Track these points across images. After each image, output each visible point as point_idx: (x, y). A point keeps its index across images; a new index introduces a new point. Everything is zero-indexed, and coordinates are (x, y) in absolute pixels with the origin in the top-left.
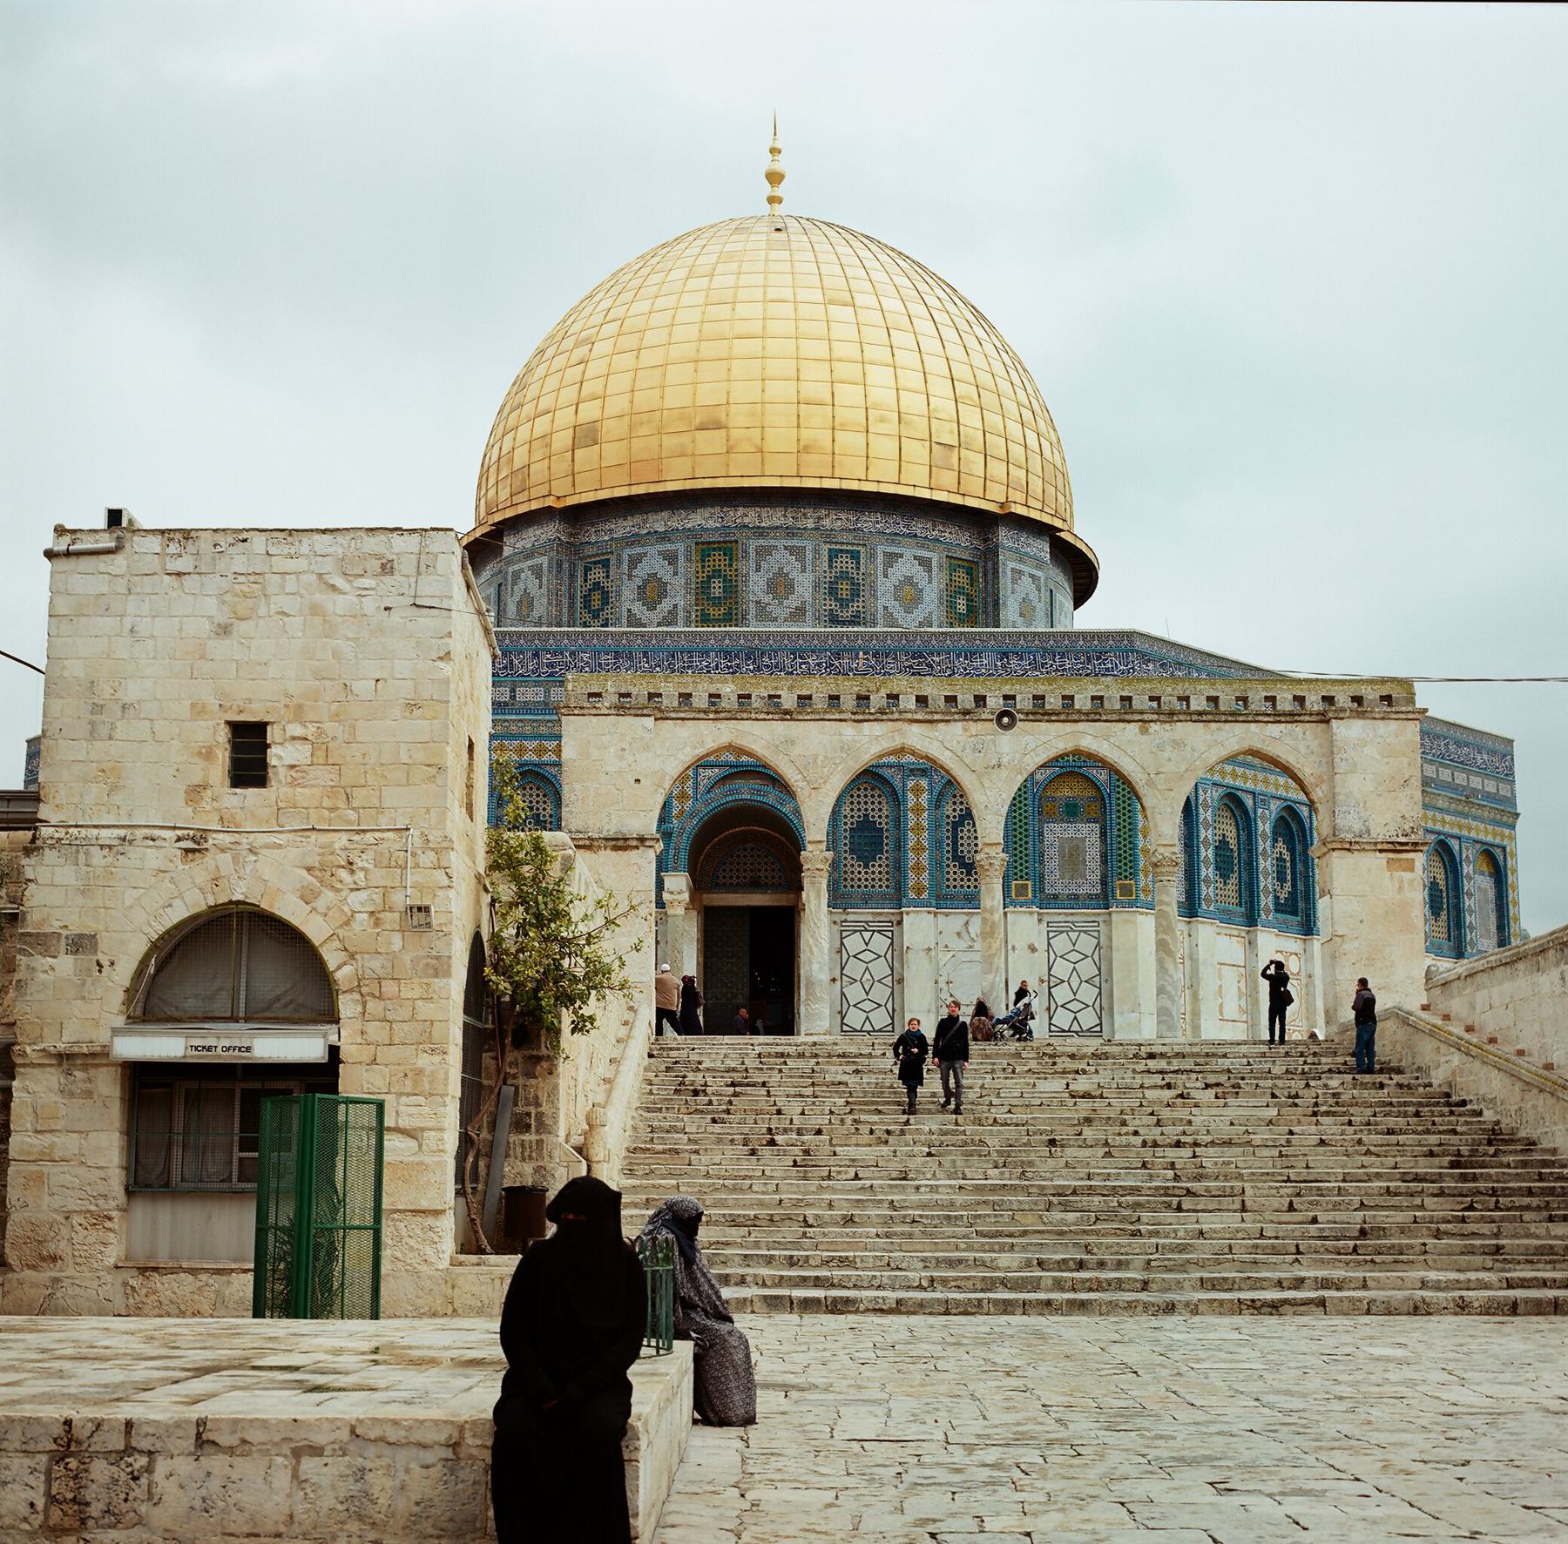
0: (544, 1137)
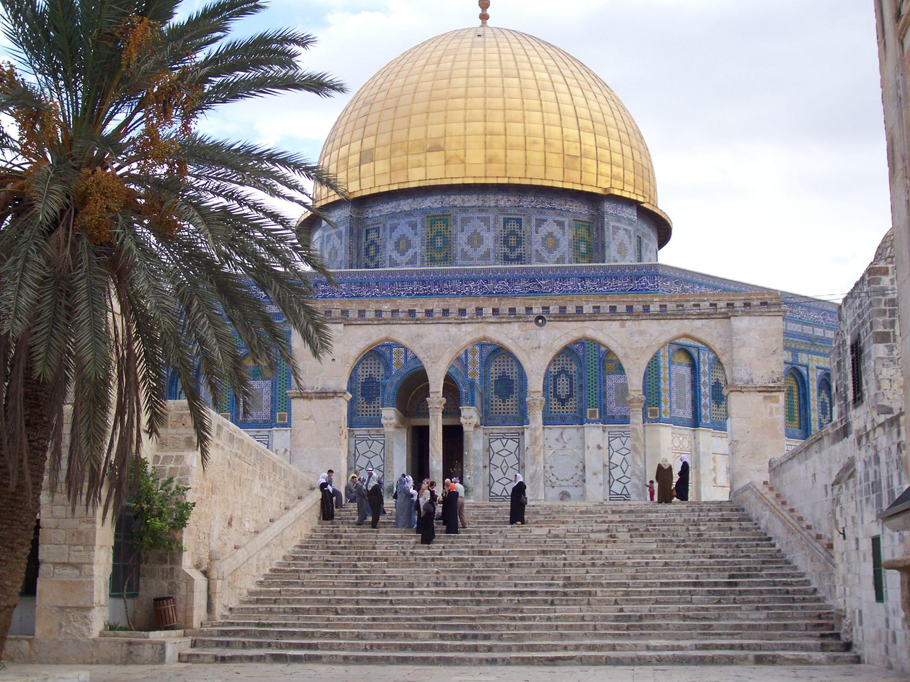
0: (174, 566)
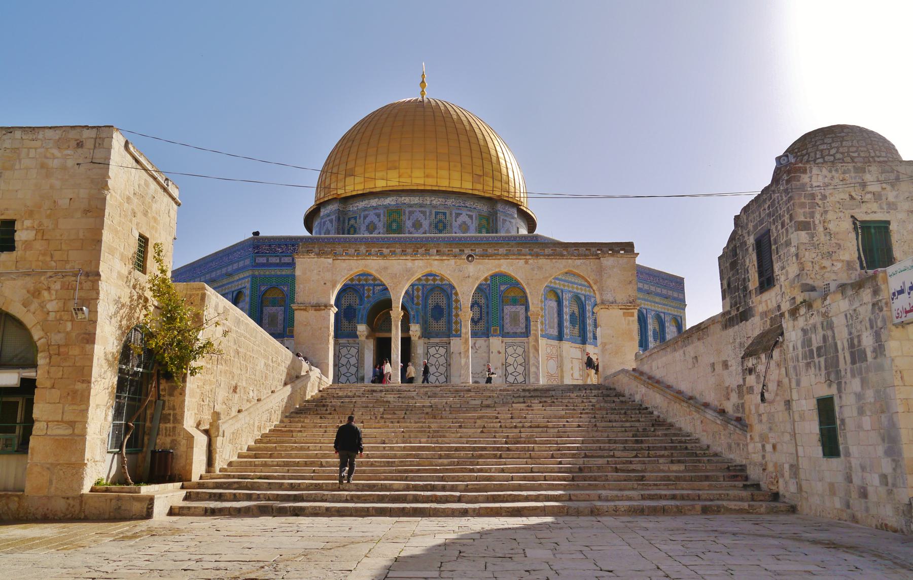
0: (177, 425)
